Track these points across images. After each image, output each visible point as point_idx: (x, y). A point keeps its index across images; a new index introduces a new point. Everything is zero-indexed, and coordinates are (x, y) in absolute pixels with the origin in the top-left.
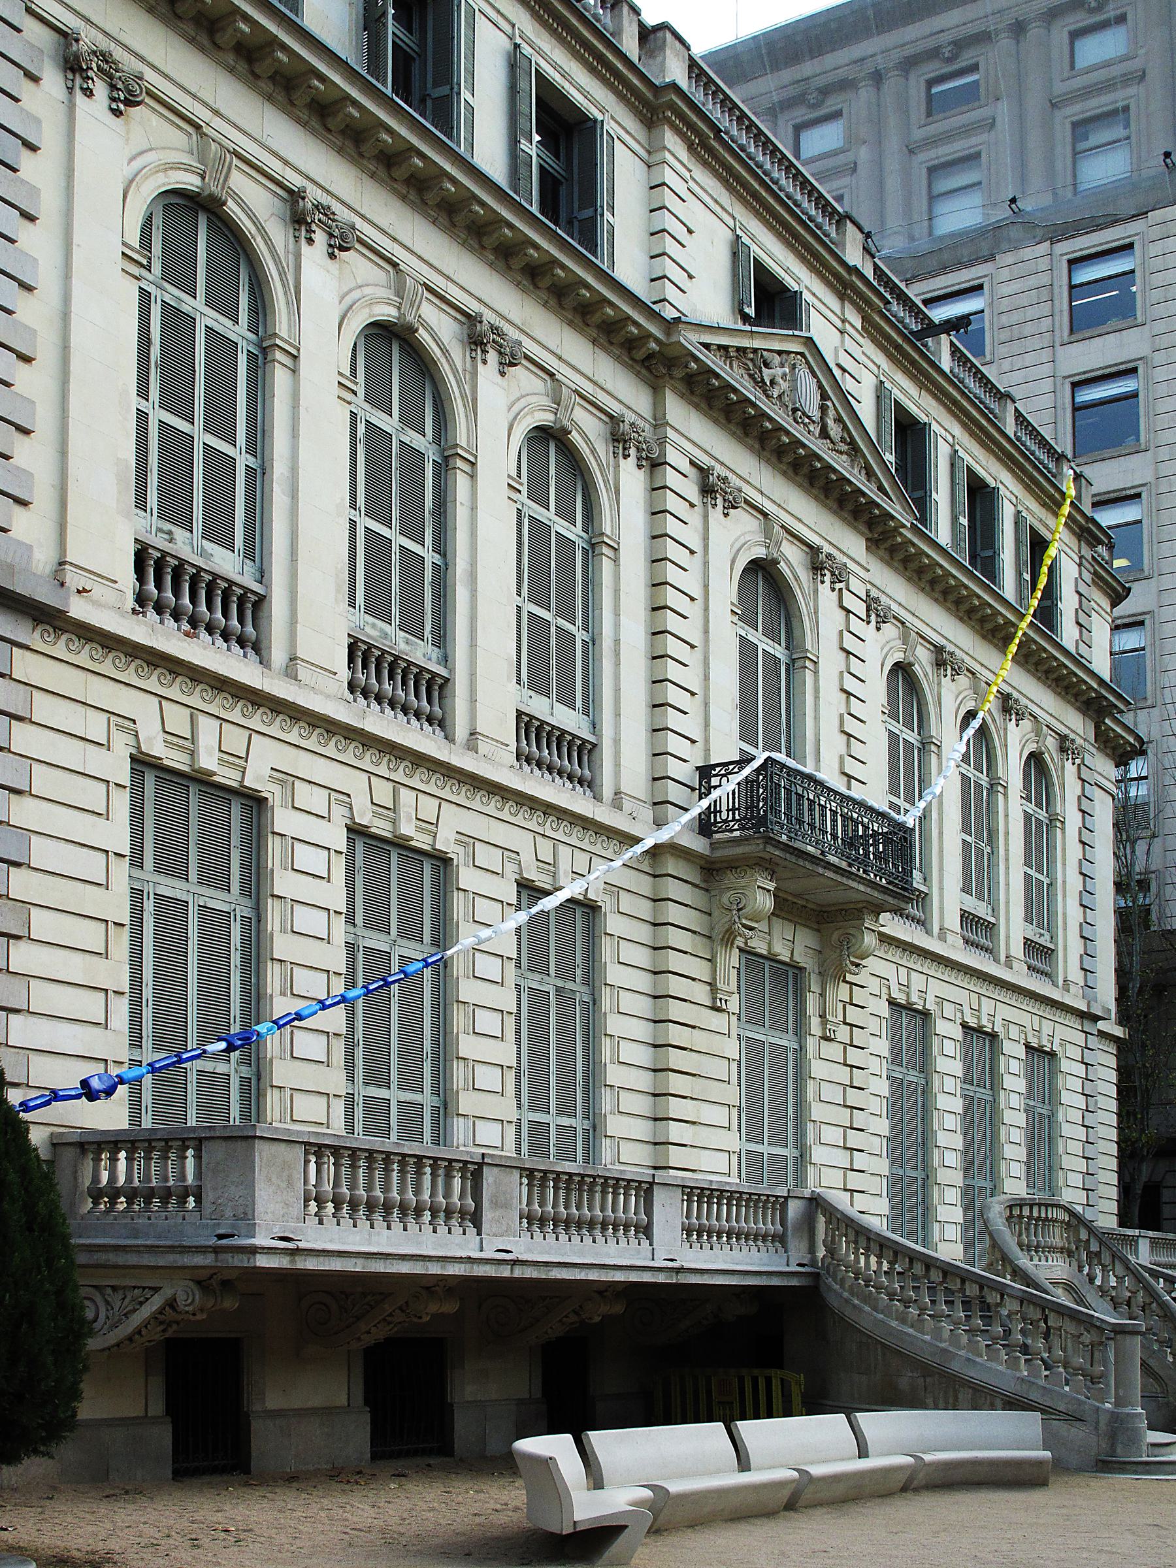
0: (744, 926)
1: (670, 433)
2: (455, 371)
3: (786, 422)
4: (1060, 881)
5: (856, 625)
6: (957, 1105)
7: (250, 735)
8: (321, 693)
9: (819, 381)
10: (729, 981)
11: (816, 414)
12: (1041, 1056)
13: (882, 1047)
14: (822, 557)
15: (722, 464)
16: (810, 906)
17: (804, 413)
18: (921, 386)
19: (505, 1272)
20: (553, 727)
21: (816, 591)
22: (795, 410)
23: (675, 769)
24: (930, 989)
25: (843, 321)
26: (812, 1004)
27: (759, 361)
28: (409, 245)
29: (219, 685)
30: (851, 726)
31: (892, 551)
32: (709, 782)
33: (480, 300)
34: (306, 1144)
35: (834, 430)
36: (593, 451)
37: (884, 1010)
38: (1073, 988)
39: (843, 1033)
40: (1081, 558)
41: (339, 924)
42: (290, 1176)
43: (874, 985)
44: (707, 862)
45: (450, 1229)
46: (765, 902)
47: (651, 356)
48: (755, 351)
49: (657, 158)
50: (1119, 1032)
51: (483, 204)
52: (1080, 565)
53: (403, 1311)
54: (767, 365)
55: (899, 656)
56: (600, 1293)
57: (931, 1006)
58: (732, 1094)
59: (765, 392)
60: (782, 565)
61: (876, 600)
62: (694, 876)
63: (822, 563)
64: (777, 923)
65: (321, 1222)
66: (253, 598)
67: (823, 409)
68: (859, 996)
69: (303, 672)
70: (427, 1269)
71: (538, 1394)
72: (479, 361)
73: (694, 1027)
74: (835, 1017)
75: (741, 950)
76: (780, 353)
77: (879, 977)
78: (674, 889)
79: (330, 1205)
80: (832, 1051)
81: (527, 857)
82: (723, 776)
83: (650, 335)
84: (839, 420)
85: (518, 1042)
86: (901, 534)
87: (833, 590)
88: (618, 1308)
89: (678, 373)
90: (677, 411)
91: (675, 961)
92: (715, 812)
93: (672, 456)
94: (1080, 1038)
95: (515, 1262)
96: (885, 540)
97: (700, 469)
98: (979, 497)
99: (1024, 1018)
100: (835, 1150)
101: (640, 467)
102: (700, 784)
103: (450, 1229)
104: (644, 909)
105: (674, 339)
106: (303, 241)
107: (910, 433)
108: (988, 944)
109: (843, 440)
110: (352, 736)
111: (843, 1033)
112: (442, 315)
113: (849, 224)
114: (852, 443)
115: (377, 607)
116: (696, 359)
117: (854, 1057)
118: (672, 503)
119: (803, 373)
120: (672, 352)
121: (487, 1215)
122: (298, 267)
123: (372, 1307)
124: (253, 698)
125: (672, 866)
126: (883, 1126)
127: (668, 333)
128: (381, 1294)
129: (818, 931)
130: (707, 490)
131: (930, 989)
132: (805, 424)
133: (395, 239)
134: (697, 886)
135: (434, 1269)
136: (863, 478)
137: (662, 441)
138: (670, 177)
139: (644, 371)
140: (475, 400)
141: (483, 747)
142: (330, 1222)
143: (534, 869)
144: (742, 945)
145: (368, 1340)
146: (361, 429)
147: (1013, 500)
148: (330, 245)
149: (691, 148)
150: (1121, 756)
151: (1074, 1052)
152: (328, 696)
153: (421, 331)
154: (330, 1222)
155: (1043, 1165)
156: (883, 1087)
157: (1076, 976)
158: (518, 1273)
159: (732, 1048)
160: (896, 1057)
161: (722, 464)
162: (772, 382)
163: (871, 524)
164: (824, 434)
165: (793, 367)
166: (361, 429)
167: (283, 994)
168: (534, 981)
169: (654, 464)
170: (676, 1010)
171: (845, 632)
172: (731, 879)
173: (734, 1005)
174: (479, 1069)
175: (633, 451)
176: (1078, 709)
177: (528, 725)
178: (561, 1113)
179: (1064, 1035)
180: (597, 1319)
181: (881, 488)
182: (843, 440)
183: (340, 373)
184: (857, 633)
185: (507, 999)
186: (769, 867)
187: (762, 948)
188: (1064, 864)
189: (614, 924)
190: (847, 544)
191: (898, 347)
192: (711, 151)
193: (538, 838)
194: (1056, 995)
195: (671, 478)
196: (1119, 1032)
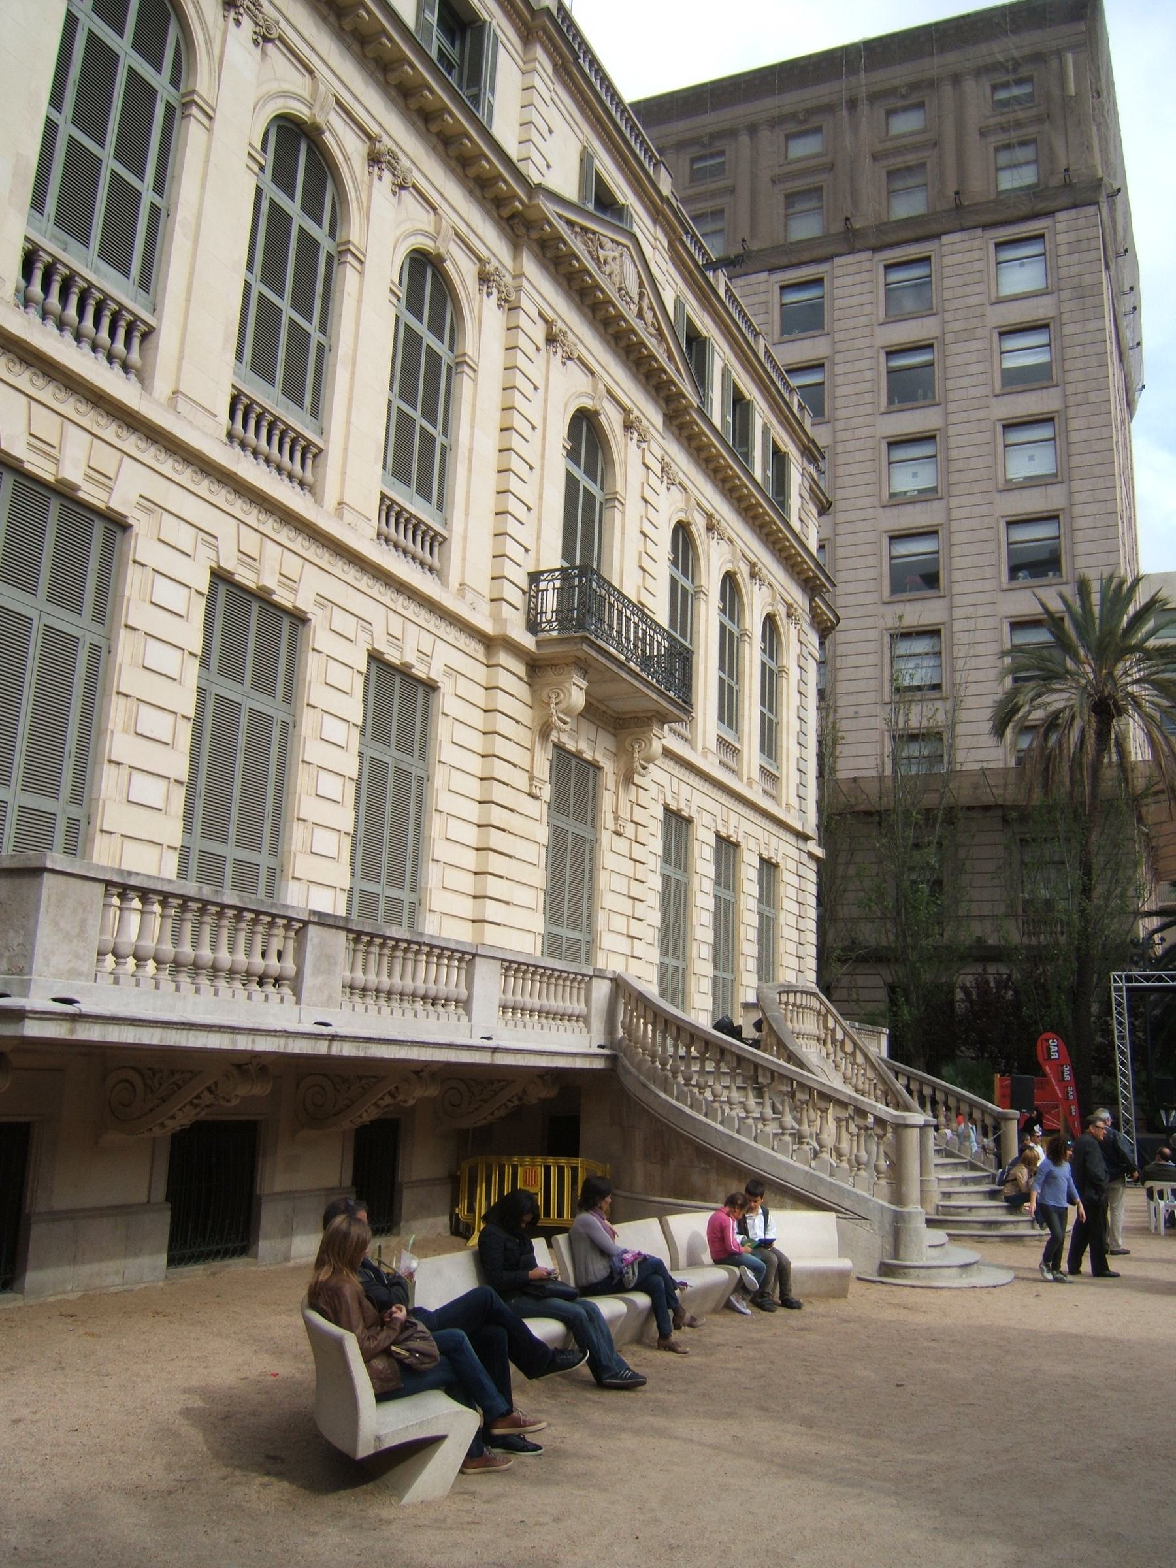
0: (559, 719)
1: (525, 283)
2: (354, 178)
3: (614, 296)
4: (784, 721)
5: (655, 481)
6: (710, 903)
7: (121, 461)
8: (198, 429)
9: (638, 273)
10: (543, 770)
11: (636, 298)
12: (768, 866)
13: (657, 845)
14: (632, 417)
15: (563, 320)
16: (610, 712)
17: (627, 293)
18: (704, 308)
19: (321, 1048)
20: (411, 515)
21: (626, 446)
22: (620, 289)
23: (510, 570)
24: (694, 799)
25: (656, 239)
26: (607, 800)
27: (597, 243)
28: (325, 57)
29: (95, 400)
30: (647, 564)
31: (681, 427)
32: (537, 586)
33: (381, 125)
34: (109, 884)
35: (648, 315)
36: (463, 282)
37: (660, 814)
38: (792, 811)
39: (629, 830)
40: (804, 469)
41: (194, 666)
42: (83, 922)
43: (654, 790)
44: (532, 659)
45: (266, 996)
46: (578, 699)
47: (514, 215)
48: (594, 233)
49: (530, 66)
50: (820, 852)
51: (391, 39)
52: (803, 475)
53: (211, 1092)
54: (602, 247)
55: (681, 516)
56: (417, 1073)
57: (694, 814)
58: (539, 877)
59: (599, 268)
60: (602, 418)
61: (668, 465)
62: (521, 669)
63: (632, 422)
64: (584, 724)
65: (116, 981)
66: (143, 328)
67: (641, 295)
68: (644, 798)
69: (182, 405)
70: (234, 1042)
71: (348, 1182)
72: (375, 177)
73: (512, 811)
74: (625, 813)
75: (555, 745)
76: (613, 241)
77: (660, 785)
78: (505, 680)
79: (131, 961)
80: (621, 845)
81: (379, 630)
82: (550, 581)
83: (515, 196)
84: (651, 308)
85: (357, 808)
86: (689, 414)
87: (639, 447)
89: (535, 235)
90: (530, 266)
91: (501, 747)
92: (542, 613)
93: (525, 303)
94: (795, 854)
95: (334, 1038)
96: (676, 417)
97: (546, 321)
98: (739, 405)
99: (759, 833)
100: (619, 937)
101: (500, 306)
102: (530, 588)
103: (266, 996)
104: (479, 696)
105: (535, 202)
106: (231, 22)
107: (696, 345)
108: (735, 766)
109: (653, 325)
110: (225, 480)
111: (629, 830)
112: (347, 128)
113: (662, 168)
114: (659, 330)
115: (262, 367)
116: (550, 224)
117: (638, 852)
118: (523, 341)
119: (628, 263)
120: (532, 215)
121: (309, 981)
122: (224, 42)
123: (179, 1087)
124: (128, 420)
125: (504, 658)
126: (655, 918)
127: (530, 198)
128: (191, 1072)
129: (615, 735)
130: (551, 339)
131: (694, 799)
132: (627, 303)
133: (313, 49)
134: (520, 678)
135: (243, 1043)
136: (665, 356)
137: (518, 289)
138: (538, 82)
139: (507, 228)
140: (369, 208)
141: (348, 516)
142: (127, 982)
143: (384, 642)
144: (556, 740)
145: (173, 1126)
146: (265, 205)
147: (762, 416)
148: (255, 33)
149: (555, 66)
150: (823, 630)
151: (792, 866)
152: (205, 434)
153: (327, 134)
154: (127, 982)
155: (766, 965)
156: (656, 882)
157: (794, 801)
158: (337, 1049)
159: (542, 834)
160: (666, 859)
161: (563, 320)
162: (605, 262)
163: (668, 400)
164: (640, 315)
165: (621, 255)
166: (265, 205)
167: (125, 731)
168: (376, 751)
169: (510, 306)
170: (499, 793)
171: (646, 485)
172: (550, 676)
173: (546, 793)
174: (318, 832)
175: (494, 291)
176: (799, 585)
177: (389, 508)
178: (390, 884)
179: (784, 850)
180: (411, 1102)
181: (678, 370)
182: (653, 325)
183: (250, 145)
184: (654, 489)
185: (350, 765)
186: (583, 666)
187: (571, 746)
188: (788, 707)
189: (447, 702)
190: (651, 415)
191: (690, 273)
192: (570, 74)
193: (390, 613)
194: (781, 815)
195: (523, 321)
196: (820, 852)
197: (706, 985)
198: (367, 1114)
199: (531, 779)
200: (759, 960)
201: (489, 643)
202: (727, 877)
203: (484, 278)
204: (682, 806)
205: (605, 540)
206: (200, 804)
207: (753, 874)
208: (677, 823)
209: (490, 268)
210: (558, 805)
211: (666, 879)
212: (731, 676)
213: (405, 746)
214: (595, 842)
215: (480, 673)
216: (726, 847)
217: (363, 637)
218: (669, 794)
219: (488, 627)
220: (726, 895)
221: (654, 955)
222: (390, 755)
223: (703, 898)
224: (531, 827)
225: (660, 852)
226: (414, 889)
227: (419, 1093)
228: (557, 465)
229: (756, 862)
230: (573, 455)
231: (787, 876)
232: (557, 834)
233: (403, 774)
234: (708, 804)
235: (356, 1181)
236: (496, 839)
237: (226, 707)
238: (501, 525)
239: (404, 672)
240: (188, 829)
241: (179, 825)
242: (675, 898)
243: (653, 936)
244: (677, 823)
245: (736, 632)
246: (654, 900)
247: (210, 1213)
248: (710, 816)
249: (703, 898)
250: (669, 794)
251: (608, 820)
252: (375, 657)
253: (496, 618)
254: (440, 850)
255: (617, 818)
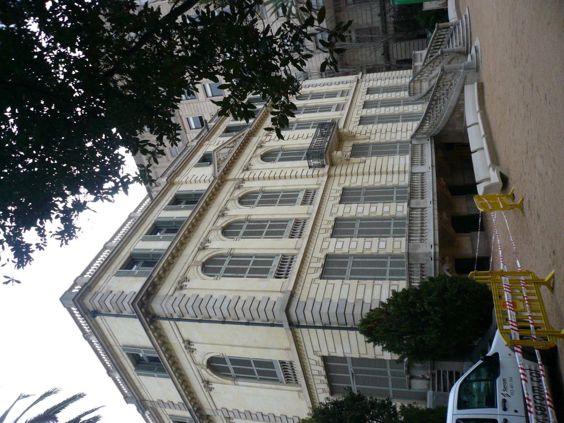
10: (358, 160)
13: (370, 126)
26: (361, 142)
57: (359, 116)
58: (385, 158)
68: (359, 132)
74: (364, 137)
77: (353, 127)
78: (338, 172)
80: (373, 137)
81: (334, 202)
88: (442, 179)
111: (368, 135)
117: (373, 132)
125: (332, 172)
126: (390, 125)
155: (397, 89)
156: (380, 125)
159: (374, 158)
170: (366, 170)
173: (364, 158)
187: (350, 153)
189: (347, 184)
197: (406, 108)
198: (448, 193)
199: (360, 163)
200: (396, 91)
201: (329, 177)
202: (374, 104)
203: (239, 187)
204: (358, 120)
205: (292, 149)
206: (382, 235)
207: (372, 96)
208: (363, 121)
209: (237, 186)
210: (366, 155)
211: (378, 123)
212: (317, 109)
213: (359, 194)
214: (373, 144)
215: (337, 178)
216: (366, 105)
217: (336, 205)
218: (356, 124)
219: (325, 178)
220: (379, 104)
221: (400, 124)
222: (362, 197)
223: (382, 111)
224: (373, 161)
225: (372, 125)
226: (393, 188)
227: (442, 182)
228: (277, 164)
229: (368, 95)
230: (274, 160)
231: (371, 85)
232: (373, 154)
233: (366, 194)
234: (355, 112)
235: (464, 194)
236: (378, 170)
237: (360, 232)
238: (298, 175)
239: (342, 195)
240: (389, 237)
241: (388, 238)
242: (383, 119)
243: (395, 125)
244: (363, 121)
245: (304, 109)
246: (385, 126)
247: (473, 223)
248: (358, 112)
249: (382, 111)
250: (356, 124)
251: (367, 141)
252: (340, 203)
253: (323, 176)
254: (383, 183)
255: (366, 139)
